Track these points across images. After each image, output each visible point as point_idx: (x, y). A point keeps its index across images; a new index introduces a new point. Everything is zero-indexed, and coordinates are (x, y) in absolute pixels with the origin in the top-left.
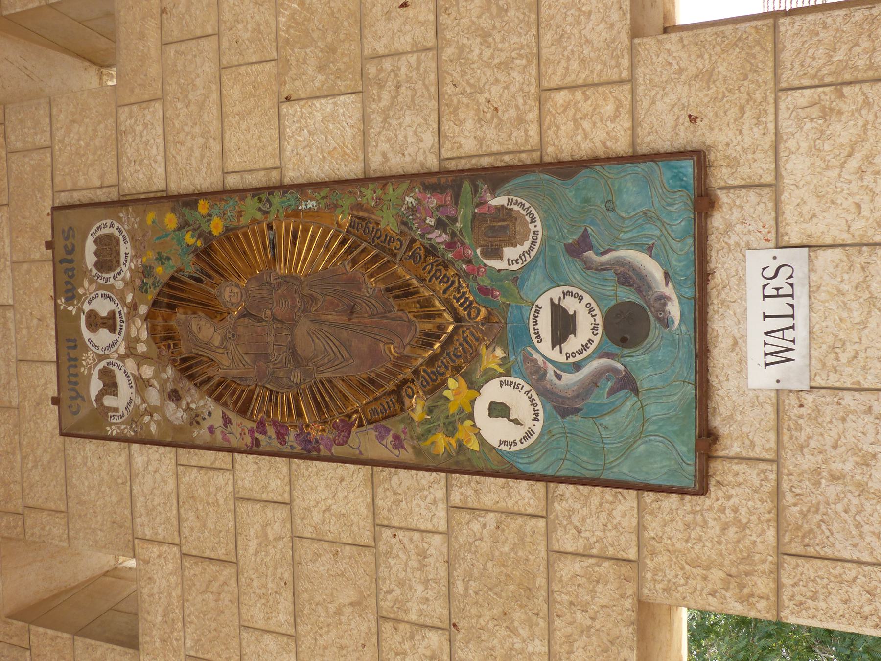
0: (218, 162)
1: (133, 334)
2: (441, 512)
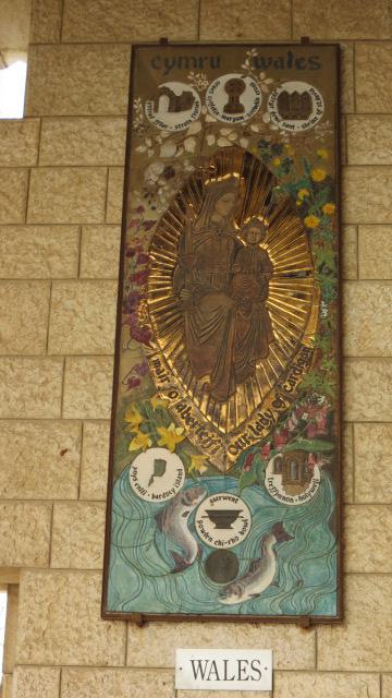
0: (367, 220)
1: (224, 132)
2: (79, 414)
